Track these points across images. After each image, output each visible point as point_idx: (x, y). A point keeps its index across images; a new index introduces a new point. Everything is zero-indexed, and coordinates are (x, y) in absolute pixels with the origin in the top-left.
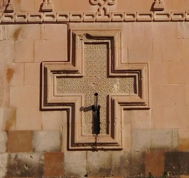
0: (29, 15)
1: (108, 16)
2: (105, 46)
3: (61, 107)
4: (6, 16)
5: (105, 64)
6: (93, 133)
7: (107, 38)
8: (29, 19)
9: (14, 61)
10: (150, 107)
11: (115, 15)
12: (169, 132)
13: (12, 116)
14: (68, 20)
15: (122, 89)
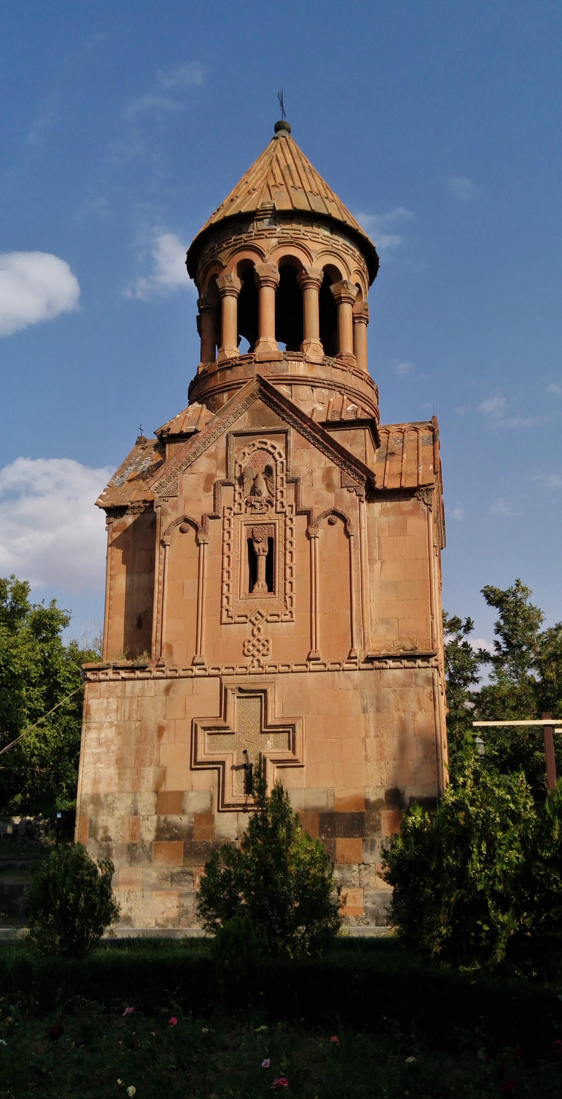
0: (181, 669)
1: (262, 667)
2: (259, 699)
3: (211, 766)
4: (157, 671)
5: (259, 718)
6: (245, 793)
7: (261, 691)
8: (182, 673)
9: (165, 718)
10: (304, 764)
11: (269, 666)
12: (324, 791)
13: (162, 777)
14: (220, 673)
15: (276, 745)
